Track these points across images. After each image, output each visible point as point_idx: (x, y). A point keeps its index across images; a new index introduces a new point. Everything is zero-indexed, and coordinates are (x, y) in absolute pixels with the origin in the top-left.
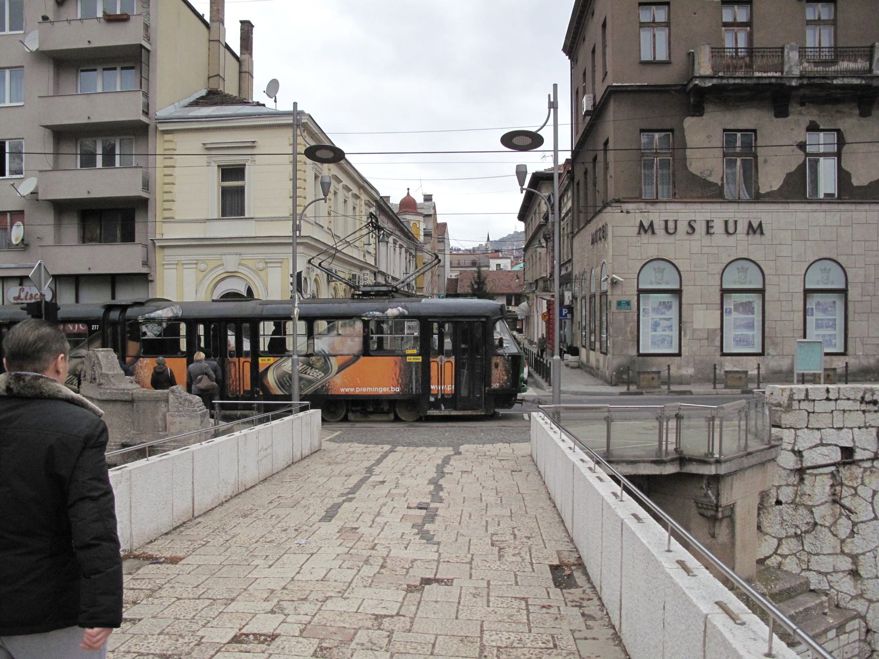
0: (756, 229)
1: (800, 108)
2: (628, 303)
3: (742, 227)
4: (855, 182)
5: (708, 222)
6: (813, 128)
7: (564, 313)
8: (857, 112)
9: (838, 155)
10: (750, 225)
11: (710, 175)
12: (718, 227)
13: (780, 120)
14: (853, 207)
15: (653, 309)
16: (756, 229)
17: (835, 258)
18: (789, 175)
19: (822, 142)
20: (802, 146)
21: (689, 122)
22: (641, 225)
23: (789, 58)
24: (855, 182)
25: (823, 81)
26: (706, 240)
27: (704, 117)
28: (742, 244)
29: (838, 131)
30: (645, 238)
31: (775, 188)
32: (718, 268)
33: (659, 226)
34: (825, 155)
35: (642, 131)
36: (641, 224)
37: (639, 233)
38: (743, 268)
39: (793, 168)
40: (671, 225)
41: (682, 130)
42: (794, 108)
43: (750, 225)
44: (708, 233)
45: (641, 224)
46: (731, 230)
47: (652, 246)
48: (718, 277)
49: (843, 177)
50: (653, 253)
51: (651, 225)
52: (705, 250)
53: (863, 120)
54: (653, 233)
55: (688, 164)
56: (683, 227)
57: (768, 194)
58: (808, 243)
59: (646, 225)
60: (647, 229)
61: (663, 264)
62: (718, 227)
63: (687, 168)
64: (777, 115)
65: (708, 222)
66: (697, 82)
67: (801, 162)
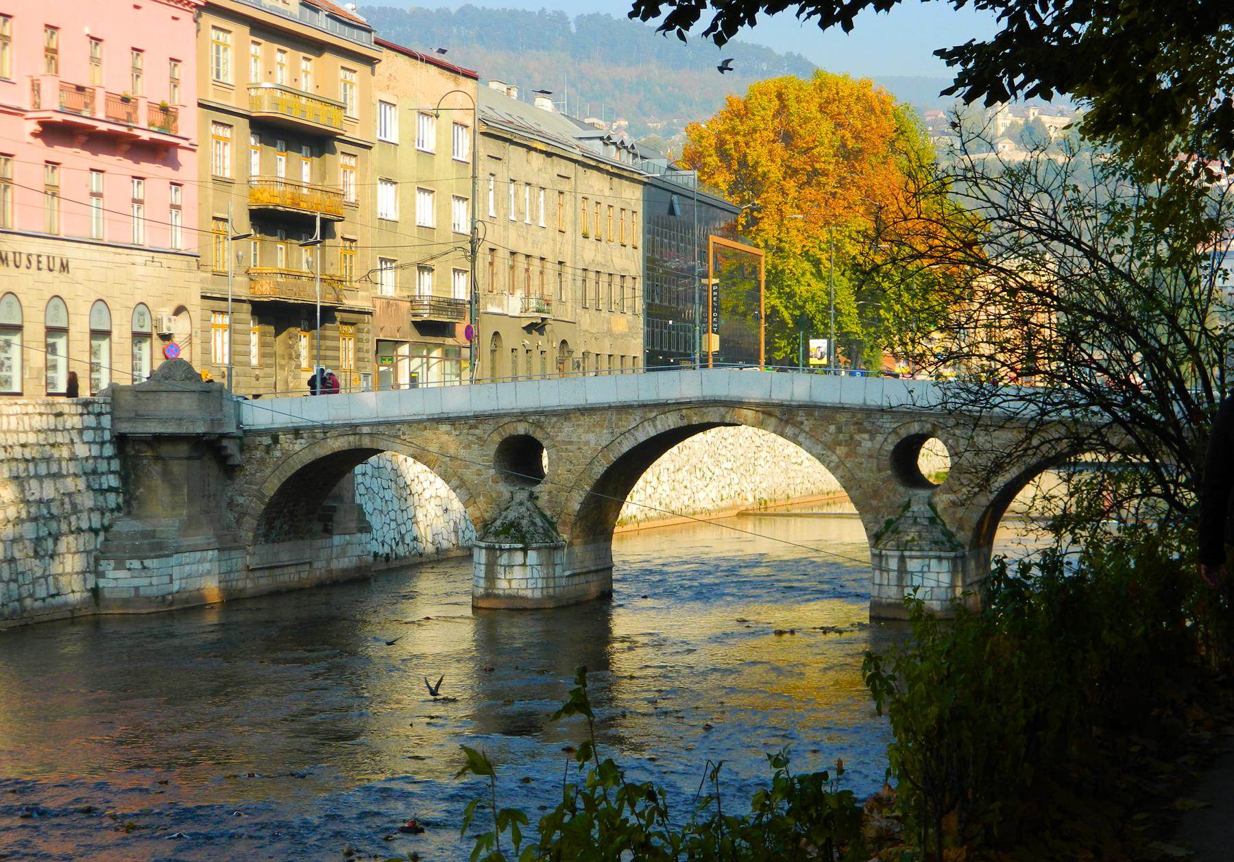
54: (8, 265)
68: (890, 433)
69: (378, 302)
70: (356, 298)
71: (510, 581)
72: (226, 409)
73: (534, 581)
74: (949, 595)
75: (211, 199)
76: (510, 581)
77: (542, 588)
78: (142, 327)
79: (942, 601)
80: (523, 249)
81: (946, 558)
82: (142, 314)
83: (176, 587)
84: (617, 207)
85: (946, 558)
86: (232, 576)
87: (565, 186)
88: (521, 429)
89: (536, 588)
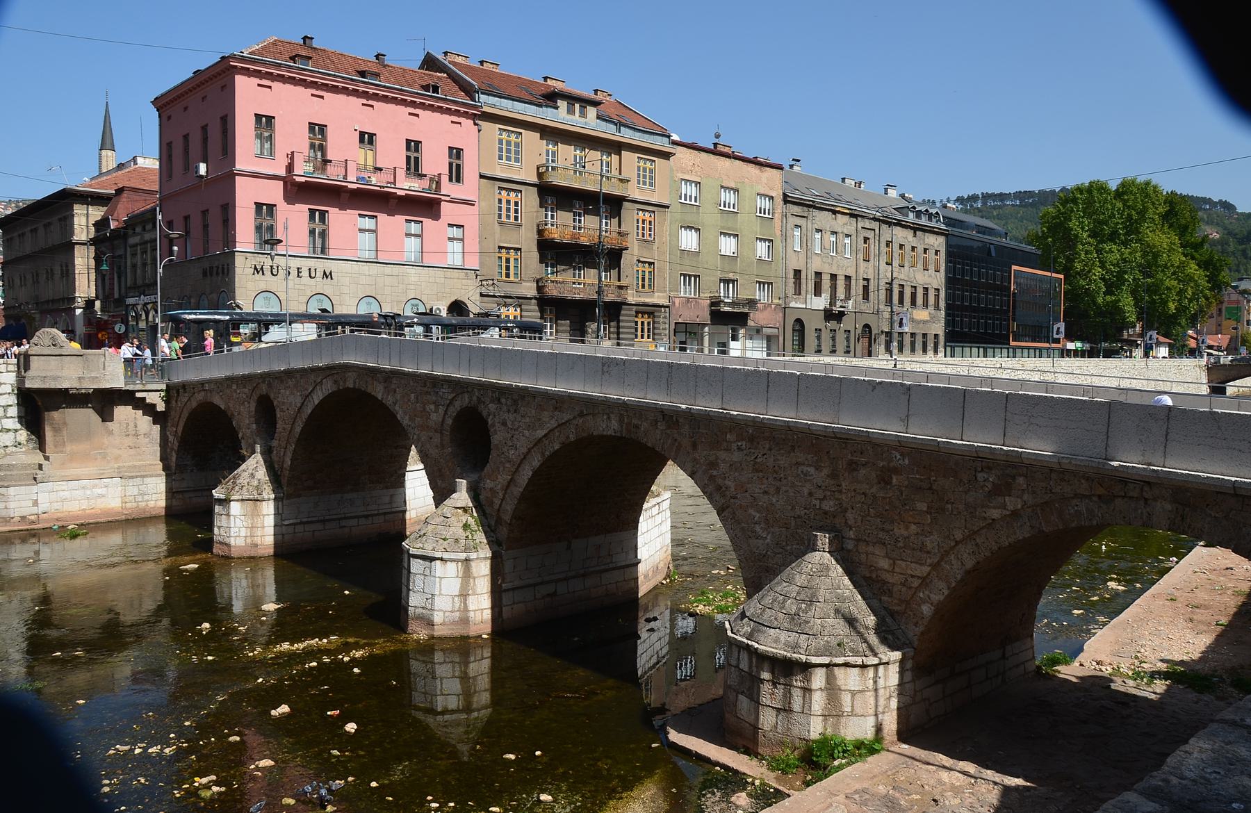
0: (327, 275)
3: (319, 274)
5: (298, 269)
10: (325, 273)
12: (305, 273)
16: (327, 275)
28: (320, 285)
30: (258, 276)
33: (267, 269)
37: (254, 274)
43: (325, 273)
44: (298, 276)
46: (313, 275)
47: (265, 281)
50: (263, 287)
52: (297, 287)
62: (305, 273)
65: (298, 269)
68: (448, 406)
69: (677, 301)
70: (653, 297)
71: (219, 527)
72: (108, 369)
73: (237, 530)
74: (457, 605)
75: (497, 236)
76: (219, 527)
77: (246, 537)
79: (445, 612)
80: (827, 270)
81: (452, 560)
83: (43, 506)
84: (920, 249)
85: (452, 560)
86: (146, 497)
87: (870, 235)
88: (264, 389)
89: (239, 536)
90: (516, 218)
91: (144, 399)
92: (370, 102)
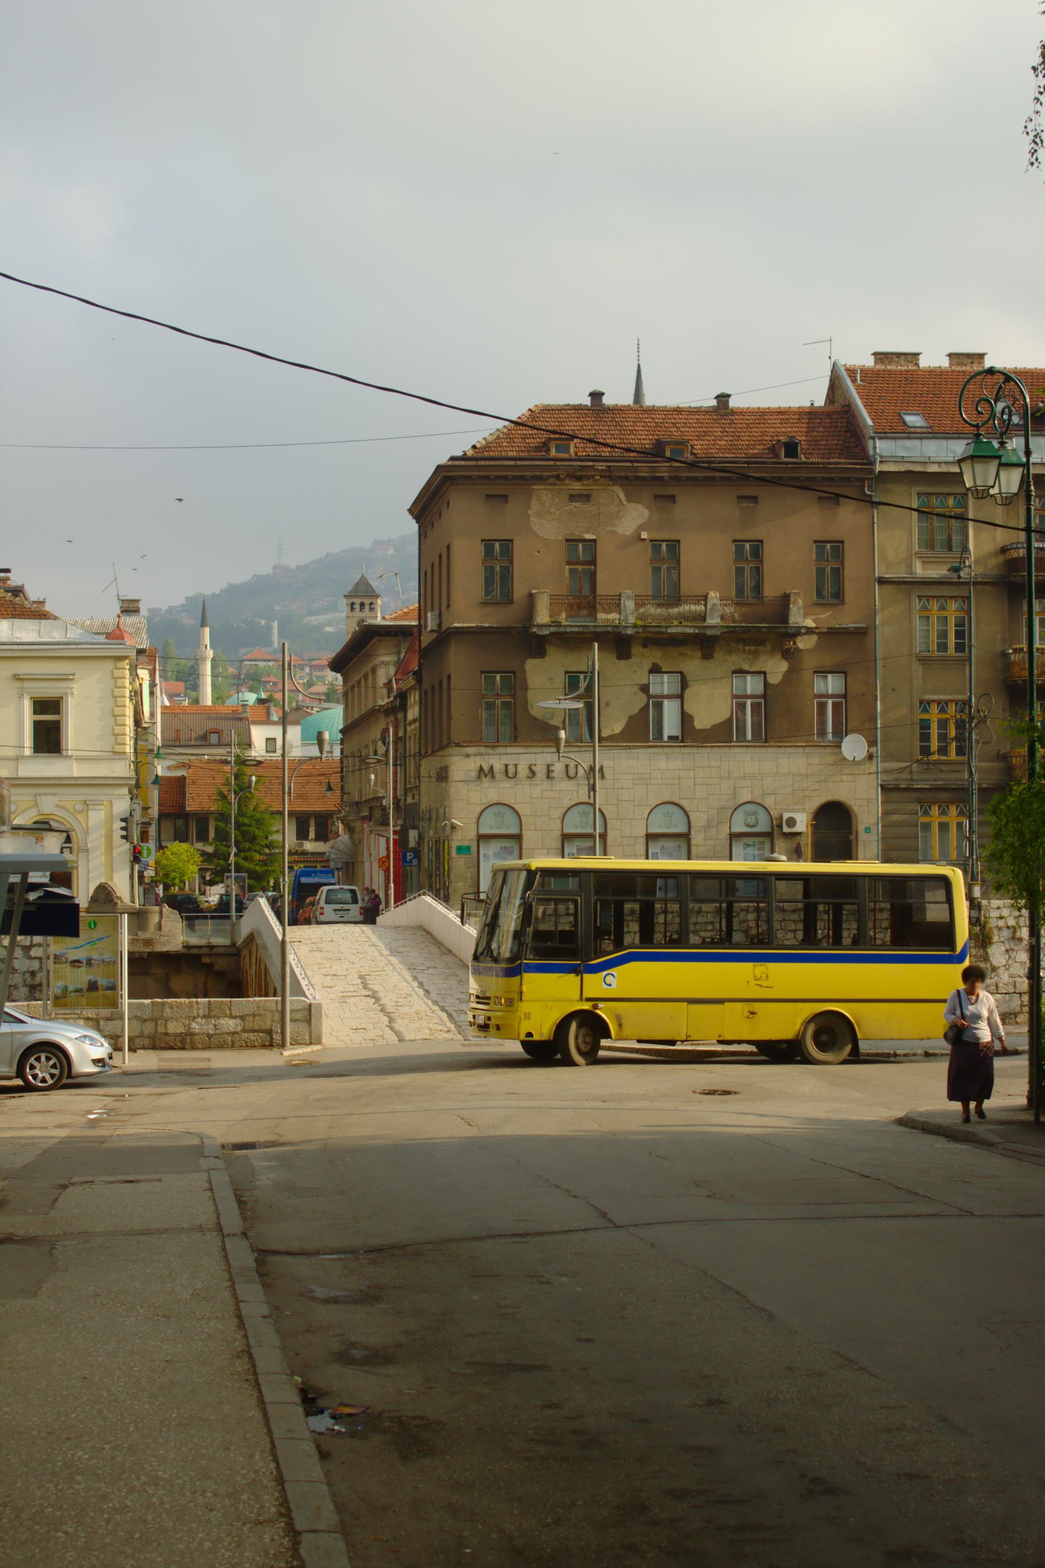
1: (642, 650)
2: (468, 848)
4: (698, 725)
5: (548, 766)
6: (656, 670)
7: (409, 858)
8: (699, 654)
9: (681, 697)
11: (551, 718)
13: (623, 663)
14: (695, 750)
15: (495, 855)
17: (677, 801)
18: (631, 718)
19: (664, 684)
20: (645, 688)
21: (532, 665)
22: (481, 768)
23: (625, 606)
24: (698, 725)
25: (658, 630)
26: (546, 785)
27: (547, 659)
29: (682, 673)
30: (486, 782)
31: (617, 731)
32: (559, 813)
34: (669, 697)
35: (482, 672)
36: (481, 767)
37: (479, 777)
38: (584, 812)
39: (635, 710)
40: (511, 769)
41: (524, 671)
42: (637, 650)
44: (548, 777)
45: (481, 767)
46: (572, 772)
47: (492, 791)
48: (559, 822)
49: (686, 719)
51: (491, 768)
52: (547, 794)
53: (706, 663)
54: (493, 777)
55: (529, 707)
56: (523, 771)
57: (612, 738)
58: (650, 787)
59: (486, 768)
60: (485, 774)
61: (503, 809)
63: (527, 708)
64: (619, 658)
65: (548, 766)
66: (534, 630)
67: (643, 704)
72: (165, 929)
78: (754, 826)
82: (755, 813)
90: (960, 648)
91: (211, 965)
92: (671, 491)
